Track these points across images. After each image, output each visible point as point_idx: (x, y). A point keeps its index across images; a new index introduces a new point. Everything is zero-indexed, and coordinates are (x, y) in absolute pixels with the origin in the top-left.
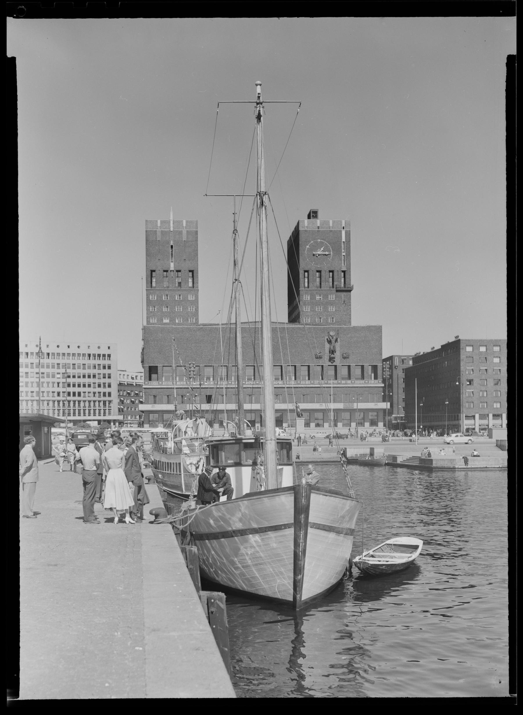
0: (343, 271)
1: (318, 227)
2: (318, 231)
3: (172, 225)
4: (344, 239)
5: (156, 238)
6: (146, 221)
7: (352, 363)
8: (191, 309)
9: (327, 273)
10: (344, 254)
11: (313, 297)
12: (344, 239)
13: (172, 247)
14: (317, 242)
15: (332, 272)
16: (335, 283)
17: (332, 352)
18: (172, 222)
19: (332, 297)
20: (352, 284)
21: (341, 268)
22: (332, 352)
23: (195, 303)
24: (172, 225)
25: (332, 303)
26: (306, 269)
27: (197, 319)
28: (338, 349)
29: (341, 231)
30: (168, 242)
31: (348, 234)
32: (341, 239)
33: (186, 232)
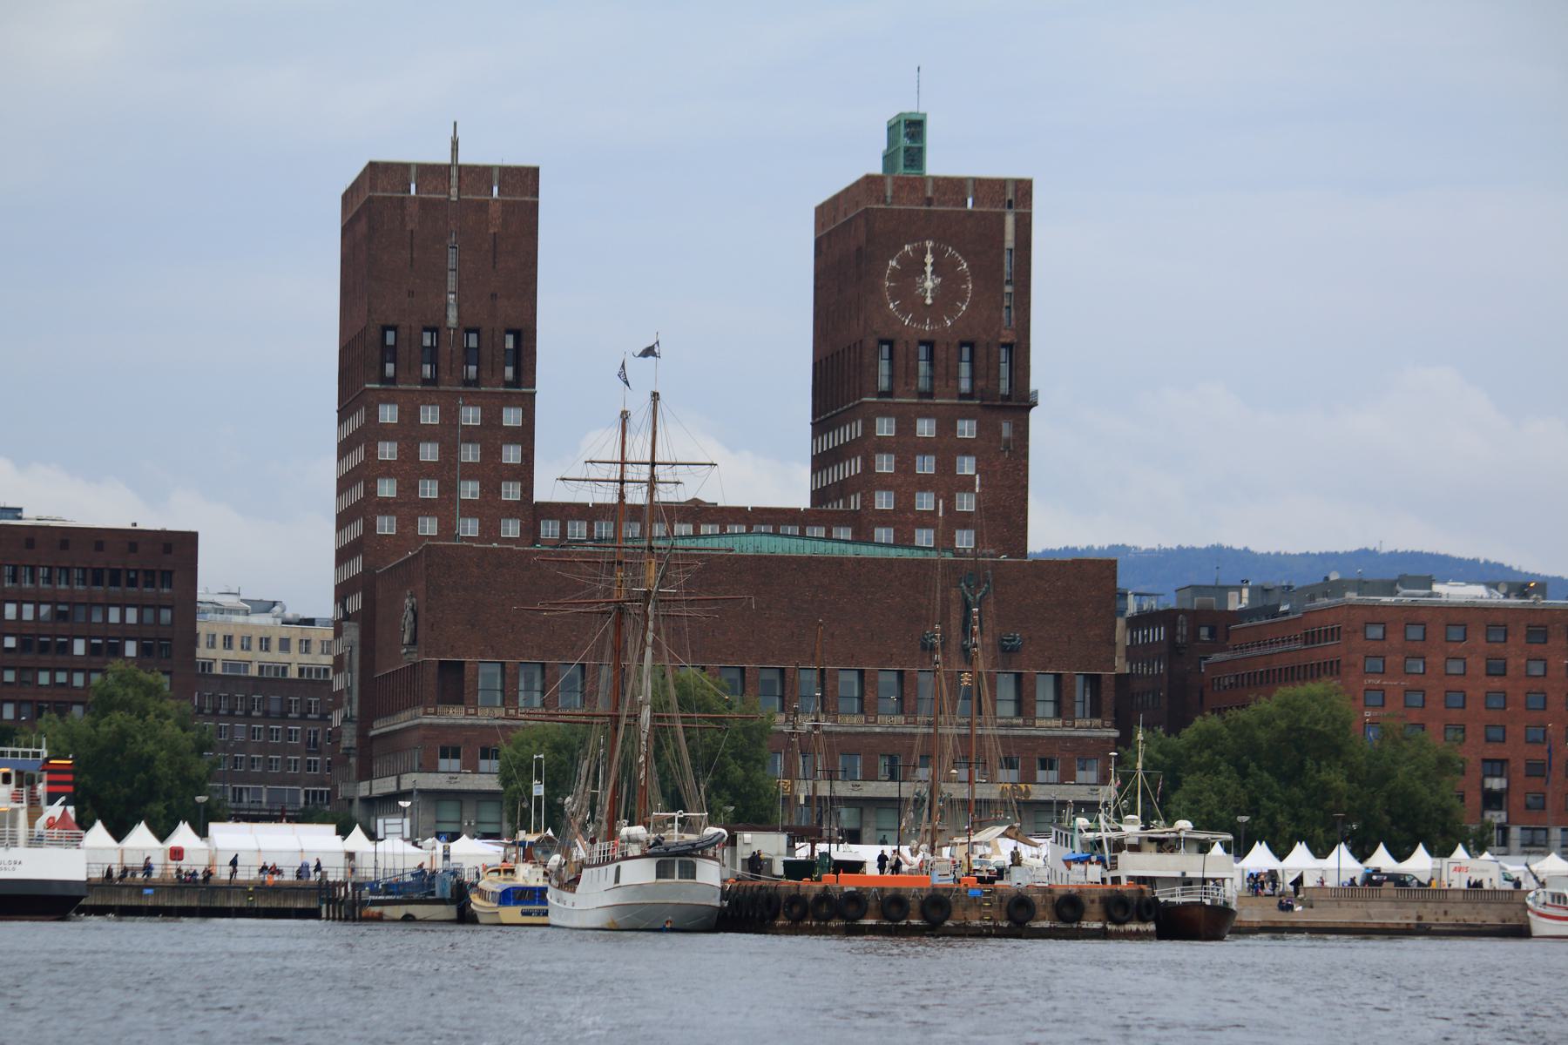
0: (1004, 345)
1: (929, 201)
3: (454, 181)
8: (512, 454)
11: (906, 428)
16: (981, 383)
18: (454, 172)
19: (966, 429)
20: (1032, 387)
21: (999, 335)
23: (525, 436)
24: (454, 181)
25: (966, 448)
26: (887, 335)
27: (528, 489)
29: (1001, 219)
32: (1003, 241)
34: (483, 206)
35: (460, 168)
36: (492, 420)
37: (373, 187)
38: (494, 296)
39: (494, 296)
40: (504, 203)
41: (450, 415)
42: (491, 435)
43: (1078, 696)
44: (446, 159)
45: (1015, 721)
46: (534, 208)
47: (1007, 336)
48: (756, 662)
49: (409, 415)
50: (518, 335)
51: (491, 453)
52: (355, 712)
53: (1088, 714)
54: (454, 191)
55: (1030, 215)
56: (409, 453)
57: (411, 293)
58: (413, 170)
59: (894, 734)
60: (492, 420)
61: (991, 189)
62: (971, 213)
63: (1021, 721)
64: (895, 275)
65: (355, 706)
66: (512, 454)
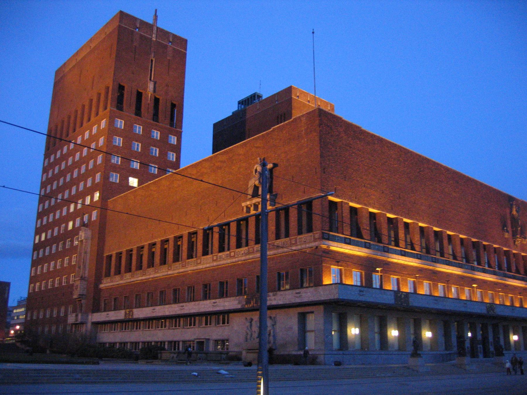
8: (172, 156)
23: (177, 149)
34: (165, 47)
35: (157, 28)
36: (164, 139)
37: (120, 21)
40: (174, 49)
41: (147, 132)
42: (164, 145)
44: (150, 21)
46: (185, 54)
49: (129, 127)
50: (173, 106)
51: (164, 154)
52: (86, 275)
54: (154, 36)
56: (127, 145)
60: (164, 139)
65: (87, 272)
66: (172, 156)
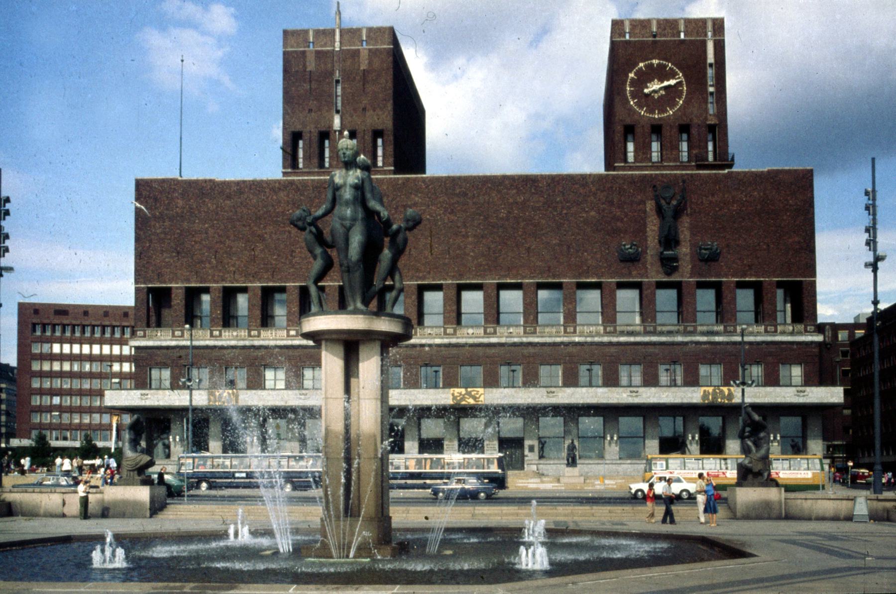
1: (655, 36)
2: (655, 42)
4: (711, 58)
5: (305, 66)
6: (285, 32)
7: (726, 276)
9: (675, 130)
10: (711, 89)
12: (711, 58)
13: (337, 82)
14: (652, 64)
15: (684, 128)
17: (669, 240)
20: (731, 150)
21: (706, 119)
22: (669, 240)
26: (628, 121)
28: (685, 234)
29: (704, 43)
30: (332, 73)
31: (720, 47)
32: (705, 58)
33: (366, 52)
34: (356, 54)
38: (364, 109)
39: (364, 109)
40: (370, 50)
43: (779, 306)
45: (716, 328)
47: (712, 121)
48: (453, 278)
53: (789, 320)
55: (723, 41)
57: (310, 111)
58: (311, 33)
59: (592, 344)
61: (698, 25)
62: (683, 41)
63: (721, 328)
64: (633, 83)
